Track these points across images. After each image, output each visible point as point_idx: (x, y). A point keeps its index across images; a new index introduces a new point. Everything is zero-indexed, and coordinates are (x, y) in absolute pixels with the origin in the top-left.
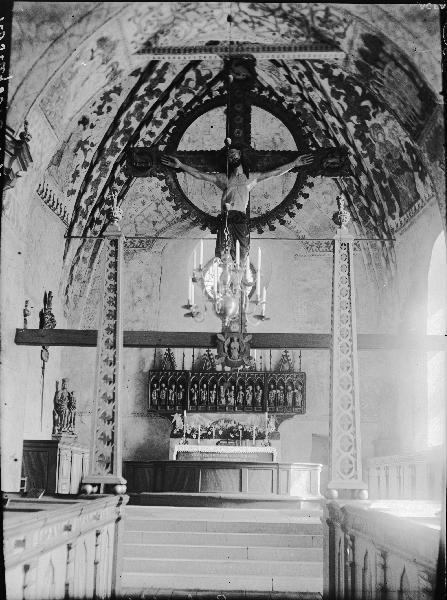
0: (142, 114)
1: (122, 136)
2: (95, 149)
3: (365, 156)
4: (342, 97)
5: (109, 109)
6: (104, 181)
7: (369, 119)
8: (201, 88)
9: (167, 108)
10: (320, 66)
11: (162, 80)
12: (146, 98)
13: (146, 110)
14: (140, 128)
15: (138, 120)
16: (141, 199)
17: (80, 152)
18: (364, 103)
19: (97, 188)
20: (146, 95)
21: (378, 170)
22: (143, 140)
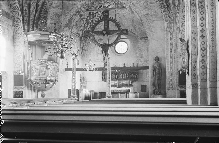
1: (92, 16)
2: (85, 20)
6: (89, 26)
14: (96, 13)
17: (82, 21)
22: (97, 16)
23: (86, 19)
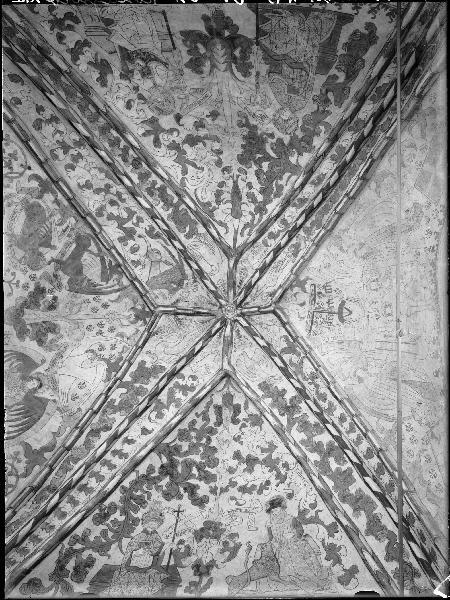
0: (316, 425)
1: (331, 460)
2: (321, 505)
3: (327, 125)
4: (280, 182)
5: (286, 465)
7: (280, 141)
9: (317, 392)
10: (257, 216)
12: (296, 416)
13: (313, 419)
15: (322, 432)
16: (423, 459)
17: (307, 528)
18: (273, 155)
19: (384, 528)
21: (330, 96)
22: (348, 432)
23: (319, 499)
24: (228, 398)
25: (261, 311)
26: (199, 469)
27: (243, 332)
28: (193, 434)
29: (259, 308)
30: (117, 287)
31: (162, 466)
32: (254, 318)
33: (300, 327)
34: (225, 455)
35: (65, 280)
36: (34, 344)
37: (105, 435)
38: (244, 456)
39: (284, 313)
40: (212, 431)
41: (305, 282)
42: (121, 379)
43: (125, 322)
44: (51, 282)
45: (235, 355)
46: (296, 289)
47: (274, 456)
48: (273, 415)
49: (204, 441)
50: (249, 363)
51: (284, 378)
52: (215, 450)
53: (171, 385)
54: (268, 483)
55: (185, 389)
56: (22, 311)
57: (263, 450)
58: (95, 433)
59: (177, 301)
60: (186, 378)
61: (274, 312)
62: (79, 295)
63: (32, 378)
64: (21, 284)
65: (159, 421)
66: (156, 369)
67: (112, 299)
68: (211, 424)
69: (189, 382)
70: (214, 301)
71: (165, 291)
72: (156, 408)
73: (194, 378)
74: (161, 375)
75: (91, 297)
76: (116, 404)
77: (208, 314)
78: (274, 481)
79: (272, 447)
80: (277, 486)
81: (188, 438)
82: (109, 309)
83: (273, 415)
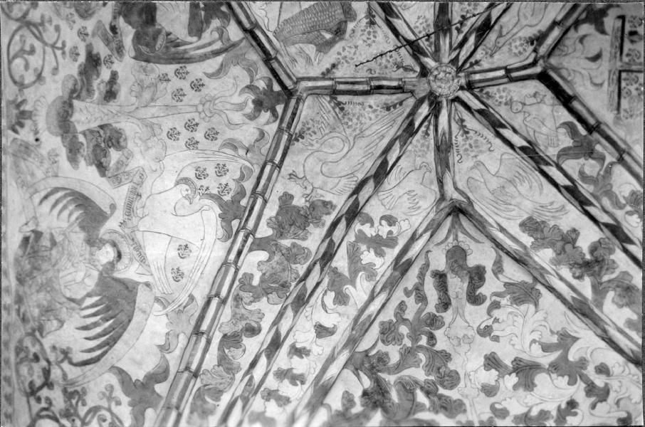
5: (603, 370)
8: (598, 148)
11: (570, 239)
12: (606, 278)
20: (596, 276)
24: (456, 255)
25: (510, 75)
26: (428, 393)
27: (472, 122)
28: (404, 330)
29: (508, 71)
30: (218, 46)
31: (365, 394)
32: (492, 90)
33: (596, 100)
34: (469, 364)
35: (128, 33)
36: (92, 171)
37: (252, 345)
38: (508, 362)
39: (562, 77)
40: (434, 321)
41: (603, 12)
42: (253, 232)
43: (237, 117)
44: (107, 42)
45: (462, 168)
46: (586, 29)
47: (573, 356)
48: (561, 279)
49: (424, 341)
50: (494, 183)
51: (570, 207)
52: (446, 357)
53: (351, 237)
54: (572, 404)
55: (379, 244)
56: (71, 106)
57: (546, 348)
58: (232, 340)
59: (334, 66)
60: (376, 224)
61: (544, 78)
62: (151, 65)
63: (103, 242)
64: (67, 49)
65: (341, 308)
66: (316, 209)
67: (210, 71)
68: (431, 308)
69: (384, 230)
70: (409, 61)
71: (311, 50)
72: (332, 286)
73: (391, 220)
74: (329, 220)
75: (170, 69)
76: (256, 282)
77: (400, 89)
78: (584, 402)
79: (566, 340)
80: (594, 406)
81: (398, 339)
82: (204, 91)
83: (561, 279)
